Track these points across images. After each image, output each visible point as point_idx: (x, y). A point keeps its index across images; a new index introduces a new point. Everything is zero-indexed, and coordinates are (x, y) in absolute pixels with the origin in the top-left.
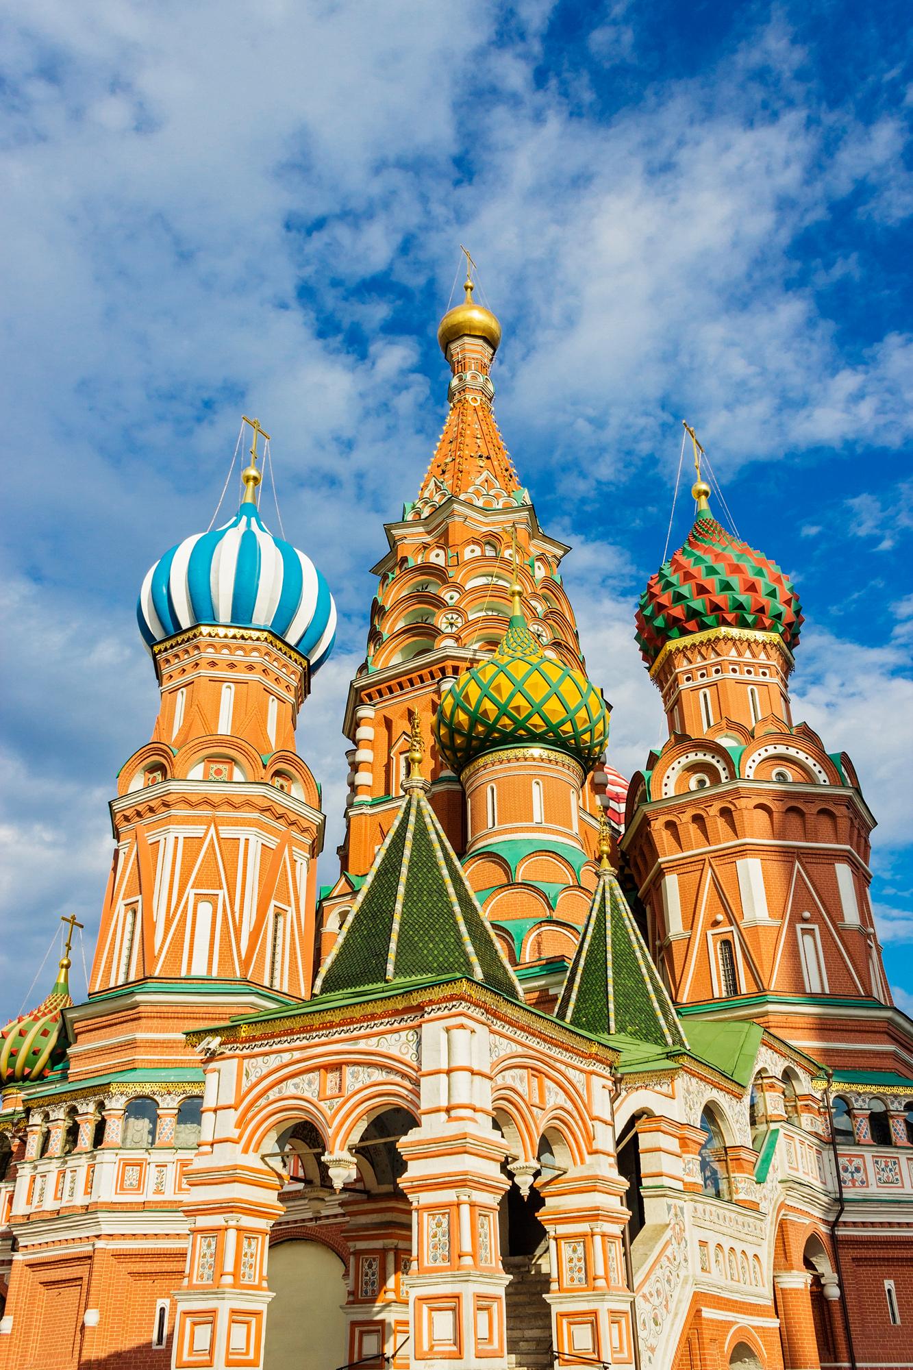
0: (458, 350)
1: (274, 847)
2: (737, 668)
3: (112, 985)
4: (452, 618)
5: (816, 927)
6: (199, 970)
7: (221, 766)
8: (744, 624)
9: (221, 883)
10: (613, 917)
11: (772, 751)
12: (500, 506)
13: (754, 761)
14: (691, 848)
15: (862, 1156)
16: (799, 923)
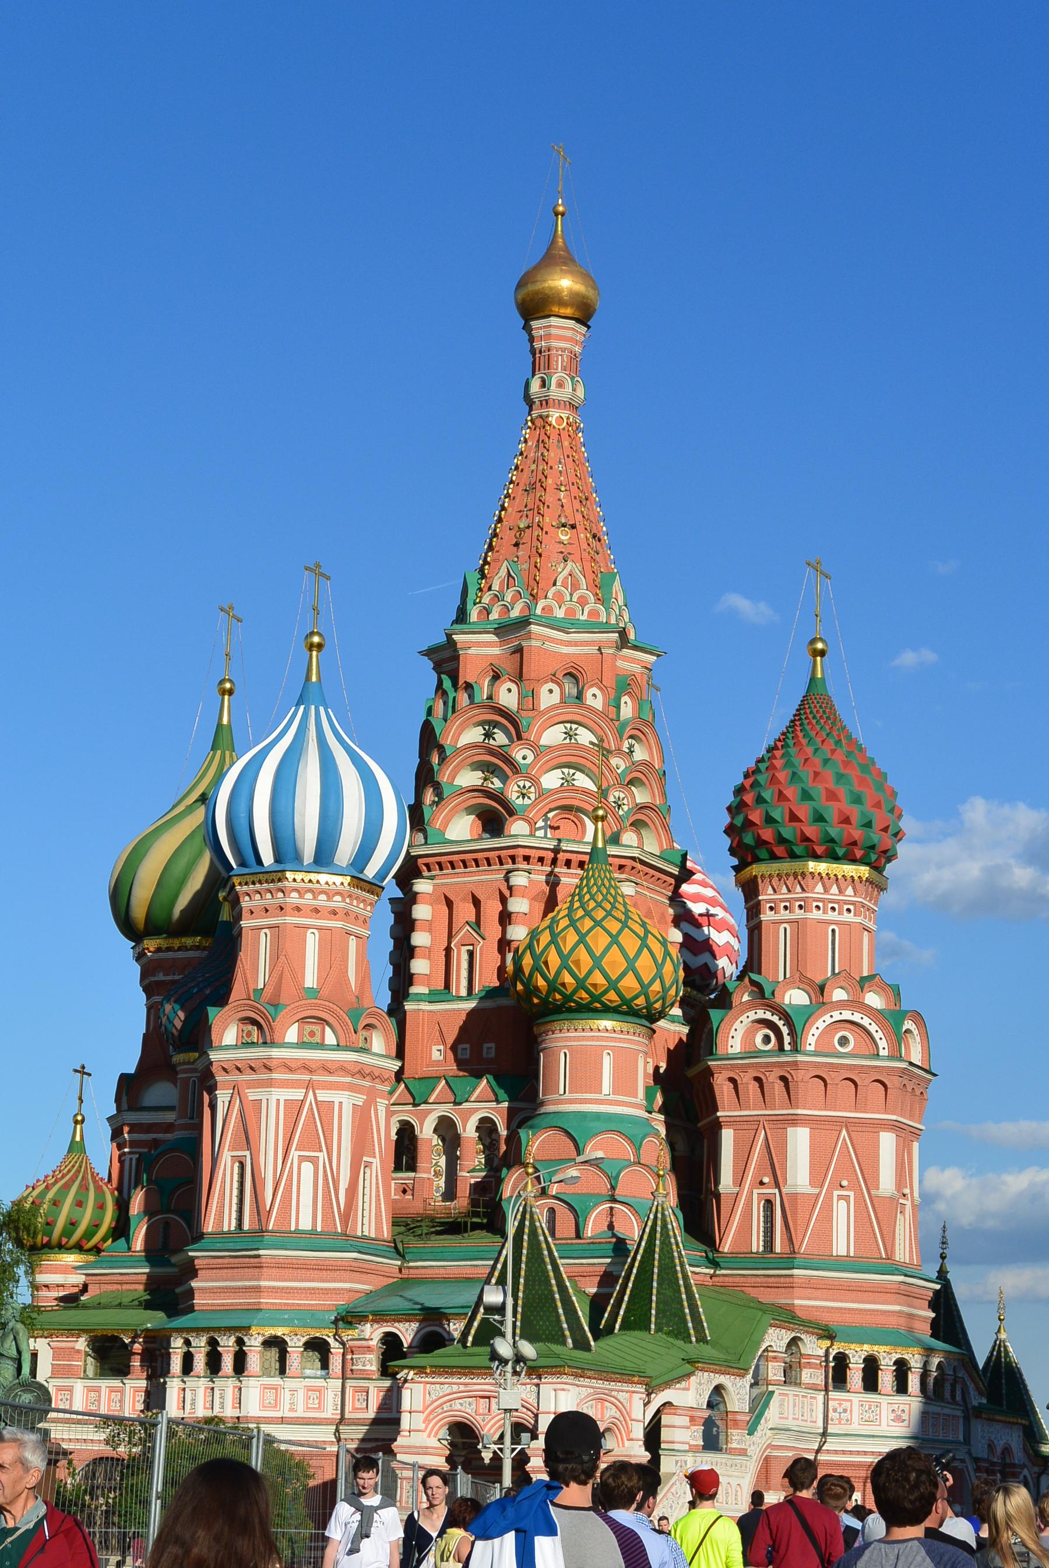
0: (542, 332)
1: (361, 1104)
2: (821, 904)
3: (226, 1229)
4: (524, 787)
5: (851, 1194)
6: (305, 1224)
7: (314, 1028)
8: (835, 858)
9: (321, 1146)
10: (662, 1235)
11: (837, 1016)
12: (584, 617)
13: (817, 1028)
14: (748, 1108)
15: (850, 1401)
16: (837, 1190)
